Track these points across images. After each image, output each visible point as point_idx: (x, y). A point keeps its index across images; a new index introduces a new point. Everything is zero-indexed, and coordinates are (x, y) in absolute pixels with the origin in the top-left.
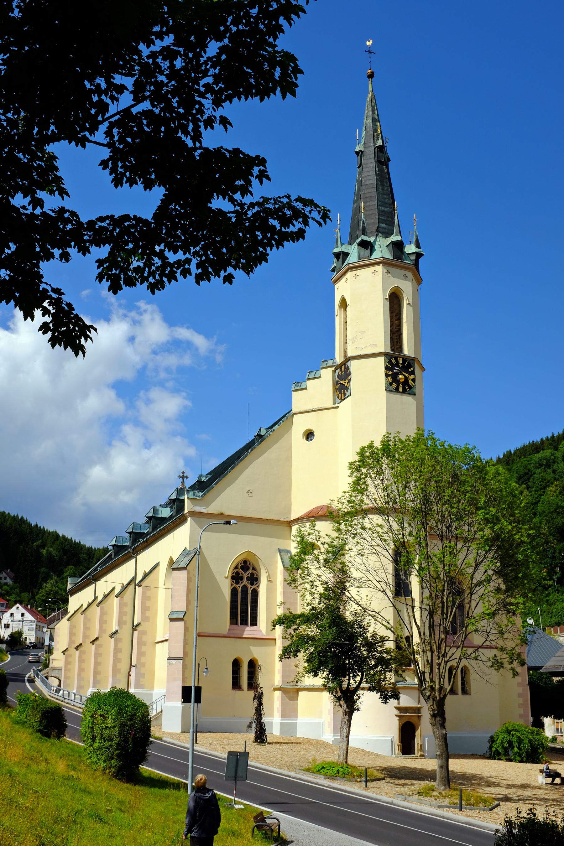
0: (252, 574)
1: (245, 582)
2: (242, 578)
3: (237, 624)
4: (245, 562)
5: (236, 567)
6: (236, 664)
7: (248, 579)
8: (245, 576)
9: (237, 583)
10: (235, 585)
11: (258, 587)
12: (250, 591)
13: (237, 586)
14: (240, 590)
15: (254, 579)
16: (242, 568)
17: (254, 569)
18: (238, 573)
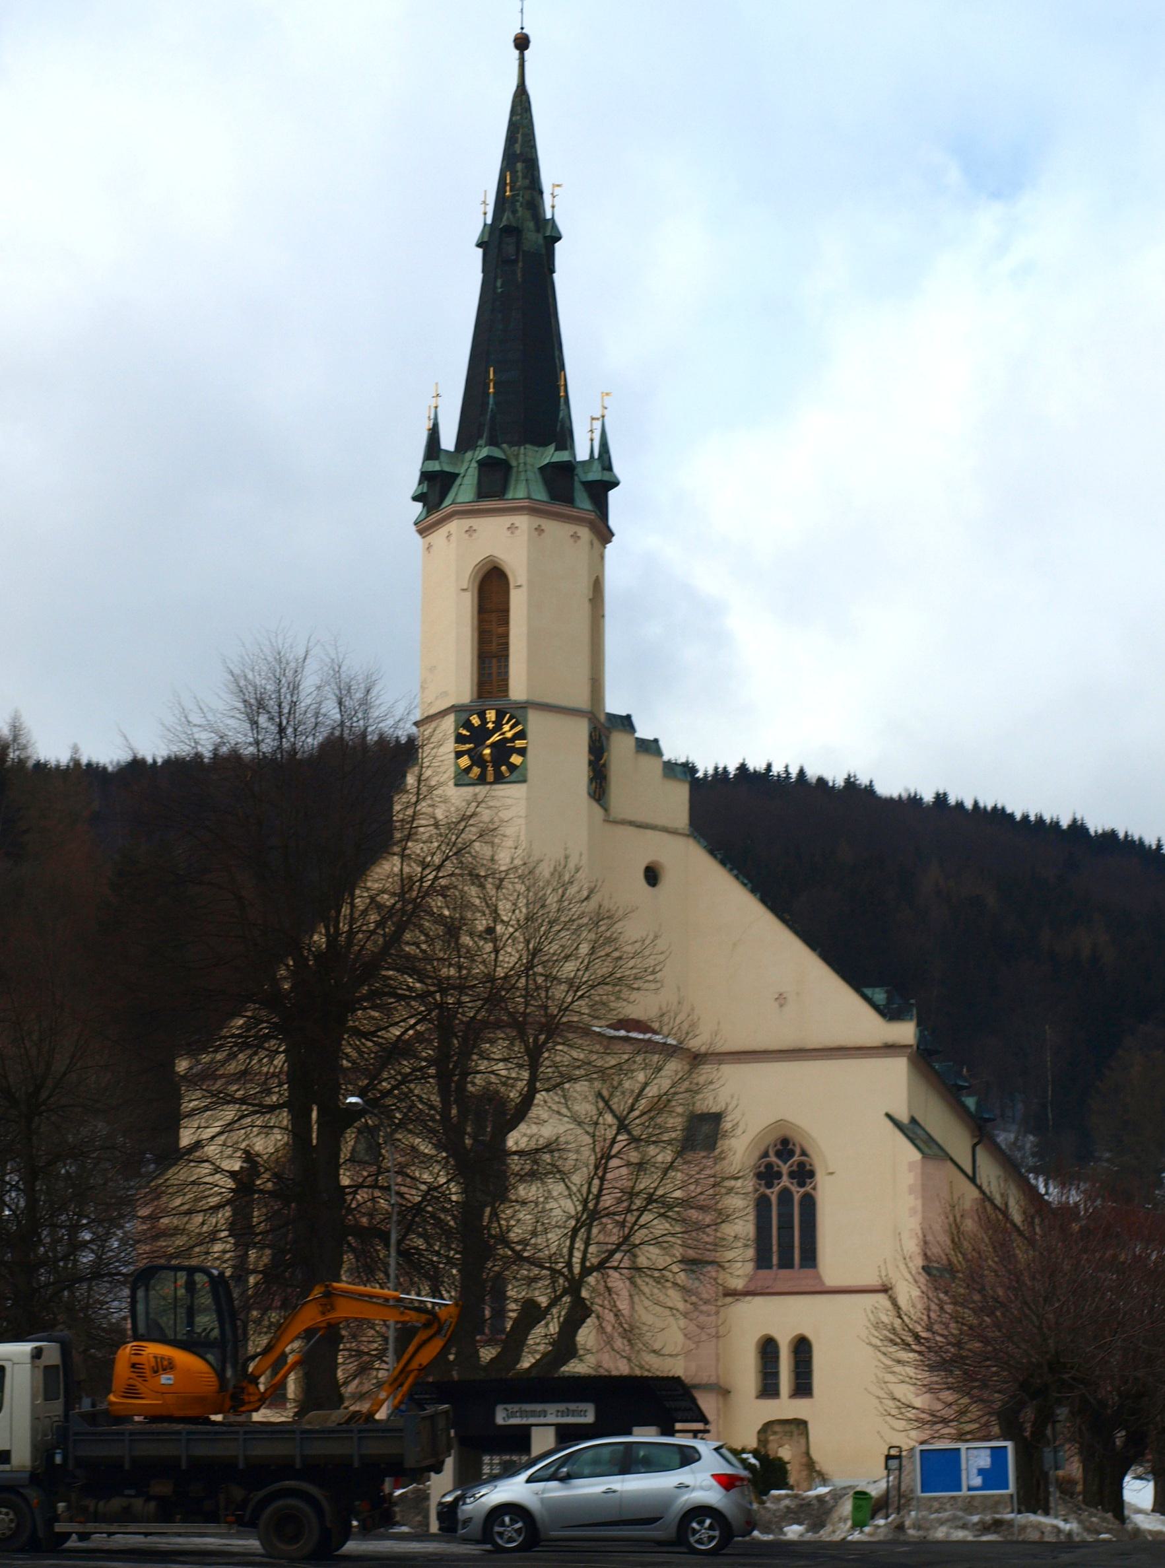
0: (801, 1165)
1: (785, 1181)
2: (779, 1175)
3: (770, 1267)
4: (785, 1141)
5: (766, 1154)
6: (768, 1348)
7: (792, 1175)
8: (785, 1169)
9: (769, 1185)
10: (762, 1189)
11: (814, 1188)
12: (797, 1198)
13: (768, 1191)
14: (774, 1199)
15: (804, 1174)
16: (778, 1154)
17: (804, 1153)
18: (769, 1166)
